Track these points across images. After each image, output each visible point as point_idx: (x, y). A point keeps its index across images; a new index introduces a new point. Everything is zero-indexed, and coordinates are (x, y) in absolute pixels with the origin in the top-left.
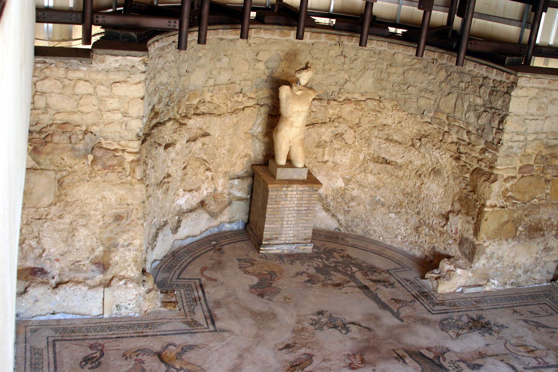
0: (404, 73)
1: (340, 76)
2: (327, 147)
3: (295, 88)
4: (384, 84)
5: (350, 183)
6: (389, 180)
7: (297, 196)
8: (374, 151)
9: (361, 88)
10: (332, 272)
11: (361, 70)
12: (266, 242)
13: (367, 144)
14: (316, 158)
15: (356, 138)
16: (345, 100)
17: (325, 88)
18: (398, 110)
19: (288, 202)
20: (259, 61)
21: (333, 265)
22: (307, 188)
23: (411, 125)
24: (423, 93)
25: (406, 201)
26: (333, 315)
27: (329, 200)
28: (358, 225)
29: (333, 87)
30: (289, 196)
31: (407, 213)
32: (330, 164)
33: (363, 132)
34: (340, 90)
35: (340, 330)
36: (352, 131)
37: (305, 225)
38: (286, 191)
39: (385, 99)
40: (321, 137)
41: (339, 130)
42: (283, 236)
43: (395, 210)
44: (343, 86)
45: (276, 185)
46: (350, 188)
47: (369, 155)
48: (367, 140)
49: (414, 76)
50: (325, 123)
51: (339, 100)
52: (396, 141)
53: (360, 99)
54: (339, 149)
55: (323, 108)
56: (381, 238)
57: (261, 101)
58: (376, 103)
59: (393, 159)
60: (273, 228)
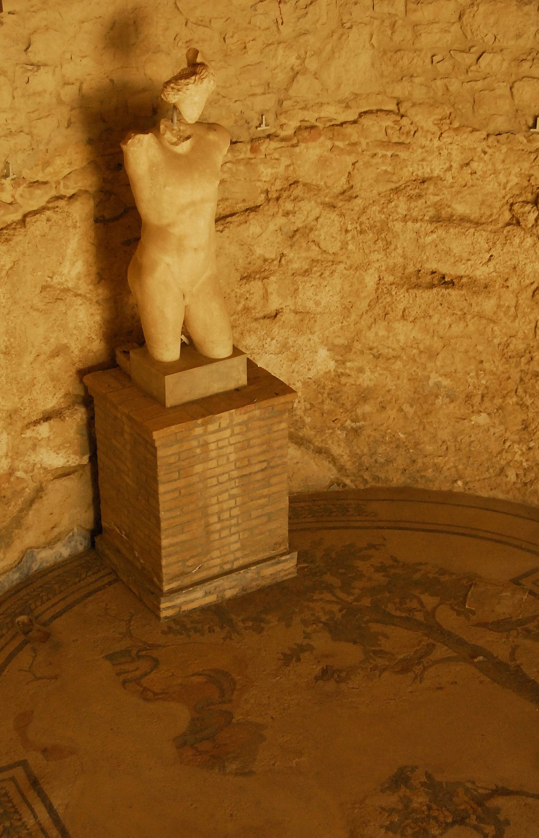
0: (460, 18)
1: (273, 64)
2: (273, 273)
3: (168, 136)
4: (406, 61)
5: (351, 356)
6: (457, 329)
7: (233, 440)
8: (404, 257)
9: (339, 86)
10: (375, 627)
11: (333, 32)
12: (174, 585)
13: (380, 244)
14: (247, 310)
15: (347, 231)
16: (299, 128)
17: (238, 107)
18: (456, 129)
19: (212, 464)
20: (38, 66)
21: (366, 602)
22: (257, 412)
23: (499, 166)
24: (526, 65)
25: (516, 375)
26: (438, 778)
27: (299, 413)
28: (389, 461)
29: (259, 99)
30: (213, 446)
31: (522, 405)
32: (287, 317)
33: (364, 211)
34: (280, 103)
35: (476, 828)
36: (334, 216)
37: (268, 509)
38: (201, 435)
39: (414, 105)
40: (251, 252)
41: (298, 221)
42: (216, 553)
43: (487, 403)
44: (286, 90)
45: (173, 428)
46: (351, 369)
47: (391, 270)
48: (380, 232)
49: (492, 20)
50: (254, 209)
51: (283, 133)
52: (463, 219)
53: (341, 118)
54: (306, 272)
55: (242, 168)
56: (460, 483)
57: (66, 187)
58: (388, 122)
59: (461, 270)
60: (183, 542)
